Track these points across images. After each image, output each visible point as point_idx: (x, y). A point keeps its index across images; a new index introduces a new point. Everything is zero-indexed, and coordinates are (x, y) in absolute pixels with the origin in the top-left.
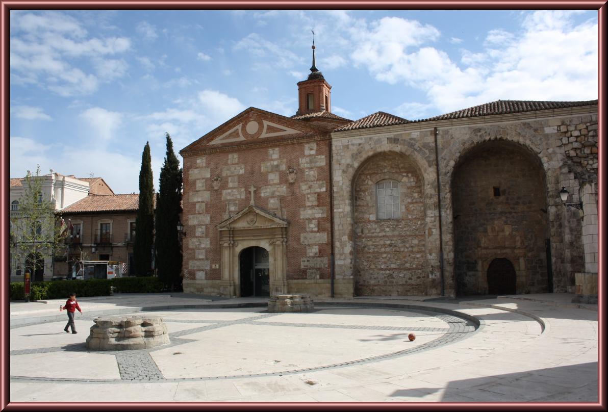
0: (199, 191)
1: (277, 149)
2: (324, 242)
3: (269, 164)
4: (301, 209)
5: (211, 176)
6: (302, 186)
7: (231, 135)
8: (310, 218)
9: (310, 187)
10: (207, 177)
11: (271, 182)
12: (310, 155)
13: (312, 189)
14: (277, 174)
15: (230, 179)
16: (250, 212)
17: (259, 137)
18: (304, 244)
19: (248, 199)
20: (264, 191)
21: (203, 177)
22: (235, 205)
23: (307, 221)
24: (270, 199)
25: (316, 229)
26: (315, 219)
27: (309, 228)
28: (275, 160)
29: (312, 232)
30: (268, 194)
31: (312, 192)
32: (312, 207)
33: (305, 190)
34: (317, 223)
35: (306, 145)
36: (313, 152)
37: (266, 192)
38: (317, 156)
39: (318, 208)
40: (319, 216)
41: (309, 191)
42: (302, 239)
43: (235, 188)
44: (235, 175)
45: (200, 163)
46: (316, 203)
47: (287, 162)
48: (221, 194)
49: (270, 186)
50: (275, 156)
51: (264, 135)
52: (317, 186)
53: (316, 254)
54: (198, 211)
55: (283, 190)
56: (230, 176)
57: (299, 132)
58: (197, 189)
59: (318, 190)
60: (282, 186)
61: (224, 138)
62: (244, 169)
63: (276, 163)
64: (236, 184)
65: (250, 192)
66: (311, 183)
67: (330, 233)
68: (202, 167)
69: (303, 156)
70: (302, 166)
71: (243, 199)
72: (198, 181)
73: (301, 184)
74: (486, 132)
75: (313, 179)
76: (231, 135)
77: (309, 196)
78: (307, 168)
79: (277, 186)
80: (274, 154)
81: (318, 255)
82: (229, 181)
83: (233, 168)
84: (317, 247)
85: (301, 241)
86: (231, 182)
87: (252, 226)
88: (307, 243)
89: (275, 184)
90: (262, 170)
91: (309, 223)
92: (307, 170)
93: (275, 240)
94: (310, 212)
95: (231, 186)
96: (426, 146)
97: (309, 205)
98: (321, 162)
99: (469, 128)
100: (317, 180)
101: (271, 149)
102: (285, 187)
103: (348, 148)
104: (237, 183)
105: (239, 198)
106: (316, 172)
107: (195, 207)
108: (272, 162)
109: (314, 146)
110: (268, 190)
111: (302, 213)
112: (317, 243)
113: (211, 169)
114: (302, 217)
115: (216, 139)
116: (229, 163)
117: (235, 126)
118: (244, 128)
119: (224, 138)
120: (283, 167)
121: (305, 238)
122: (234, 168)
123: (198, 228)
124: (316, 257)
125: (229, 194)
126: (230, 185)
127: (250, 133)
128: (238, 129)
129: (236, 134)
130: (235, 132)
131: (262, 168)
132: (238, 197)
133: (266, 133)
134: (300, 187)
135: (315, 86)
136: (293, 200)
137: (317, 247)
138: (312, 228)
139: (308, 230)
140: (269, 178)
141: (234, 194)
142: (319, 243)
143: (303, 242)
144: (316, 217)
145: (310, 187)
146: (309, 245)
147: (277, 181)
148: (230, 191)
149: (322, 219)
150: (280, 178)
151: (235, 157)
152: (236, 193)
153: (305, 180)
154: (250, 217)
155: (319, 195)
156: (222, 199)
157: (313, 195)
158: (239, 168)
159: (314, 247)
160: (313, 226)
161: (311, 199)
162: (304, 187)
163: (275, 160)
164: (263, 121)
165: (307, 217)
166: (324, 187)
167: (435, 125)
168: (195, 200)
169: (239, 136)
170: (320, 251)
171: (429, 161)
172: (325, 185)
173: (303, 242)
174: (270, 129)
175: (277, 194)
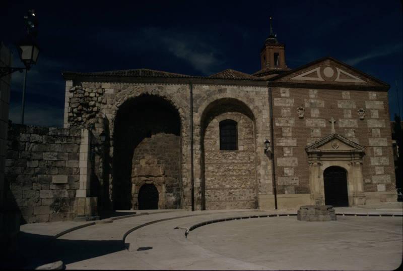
16: (335, 138)
19: (328, 128)
55: (355, 123)
57: (362, 81)
61: (304, 76)
65: (331, 122)
69: (368, 99)
71: (324, 128)
80: (346, 94)
87: (335, 149)
93: (312, 162)
118: (322, 70)
119: (304, 76)
128: (316, 71)
135: (281, 49)
136: (364, 132)
141: (316, 123)
154: (334, 142)
164: (337, 69)
174: (342, 76)
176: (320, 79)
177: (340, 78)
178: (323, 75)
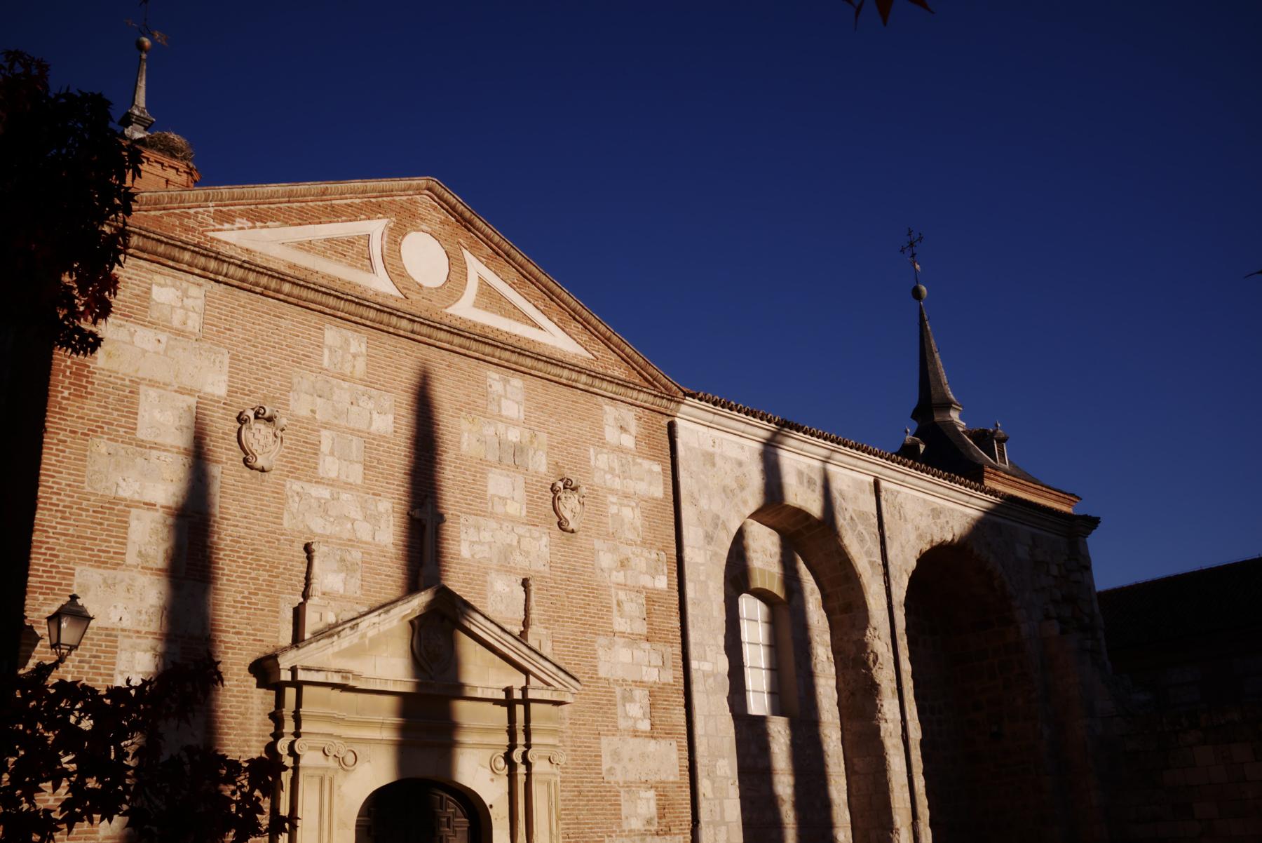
0: (155, 446)
1: (517, 382)
2: (671, 779)
3: (489, 431)
4: (602, 640)
5: (231, 393)
6: (601, 553)
7: (336, 248)
8: (629, 679)
9: (624, 564)
10: (209, 389)
11: (499, 509)
12: (619, 449)
13: (629, 573)
14: (520, 480)
15: (326, 438)
17: (449, 311)
18: (612, 779)
20: (472, 535)
21: (187, 382)
22: (346, 566)
23: (618, 691)
24: (493, 575)
25: (645, 725)
26: (640, 683)
27: (627, 716)
28: (510, 422)
29: (636, 734)
30: (482, 552)
31: (629, 583)
32: (632, 640)
33: (611, 570)
34: (646, 702)
35: (607, 408)
36: (628, 441)
37: (480, 543)
38: (639, 460)
39: (647, 646)
40: (652, 675)
41: (619, 577)
42: (606, 763)
43: (348, 486)
44: (354, 432)
45: (173, 307)
46: (641, 628)
47: (551, 447)
48: (280, 497)
49: (494, 525)
50: (512, 409)
51: (466, 310)
52: (642, 565)
53: (649, 822)
54: (140, 554)
56: (326, 426)
58: (141, 434)
59: (646, 581)
60: (536, 532)
62: (391, 417)
63: (514, 435)
64: (356, 474)
66: (627, 551)
67: (685, 743)
68: (180, 333)
69: (602, 444)
70: (597, 479)
72: (153, 393)
73: (598, 544)
74: (947, 522)
75: (630, 535)
76: (336, 248)
77: (622, 595)
78: (613, 491)
79: (521, 530)
81: (654, 828)
82: (325, 447)
83: (343, 394)
84: (652, 794)
85: (605, 767)
86: (332, 454)
88: (619, 777)
89: (513, 520)
90: (464, 447)
91: (624, 698)
92: (613, 499)
94: (623, 654)
95: (333, 475)
96: (863, 515)
97: (623, 629)
98: (650, 484)
99: (925, 501)
100: (644, 543)
101: (496, 376)
102: (545, 540)
103: (714, 465)
104: (359, 469)
105: (367, 537)
106: (638, 511)
107: (124, 525)
108: (501, 427)
109: (629, 416)
110: (486, 536)
111: (601, 652)
112: (654, 778)
113: (233, 358)
114: (601, 674)
115: (265, 231)
116: (326, 363)
117: (354, 218)
120: (540, 463)
121: (616, 755)
122: (347, 398)
123: (134, 647)
124: (652, 835)
125: (324, 508)
126: (329, 467)
127: (417, 279)
129: (355, 250)
130: (350, 242)
131: (466, 434)
132: (364, 531)
133: (474, 306)
134: (594, 552)
137: (652, 794)
138: (636, 720)
139: (623, 724)
140: (491, 490)
142: (658, 779)
143: (611, 770)
144: (645, 679)
145: (624, 564)
146: (628, 785)
147: (516, 508)
148: (324, 493)
149: (663, 687)
150: (530, 502)
151: (353, 350)
152: (355, 513)
153: (607, 535)
155: (651, 599)
156: (287, 523)
157: (633, 595)
158: (371, 405)
159: (643, 794)
160: (636, 711)
161: (627, 607)
162: (606, 560)
163: (510, 422)
164: (467, 255)
165: (619, 674)
166: (663, 574)
167: (879, 469)
168: (128, 491)
169: (371, 268)
170: (661, 816)
171: (872, 564)
172: (665, 568)
173: (611, 770)
174: (489, 297)
175: (519, 560)
176: (379, 284)
177: (476, 305)
178: (397, 272)
